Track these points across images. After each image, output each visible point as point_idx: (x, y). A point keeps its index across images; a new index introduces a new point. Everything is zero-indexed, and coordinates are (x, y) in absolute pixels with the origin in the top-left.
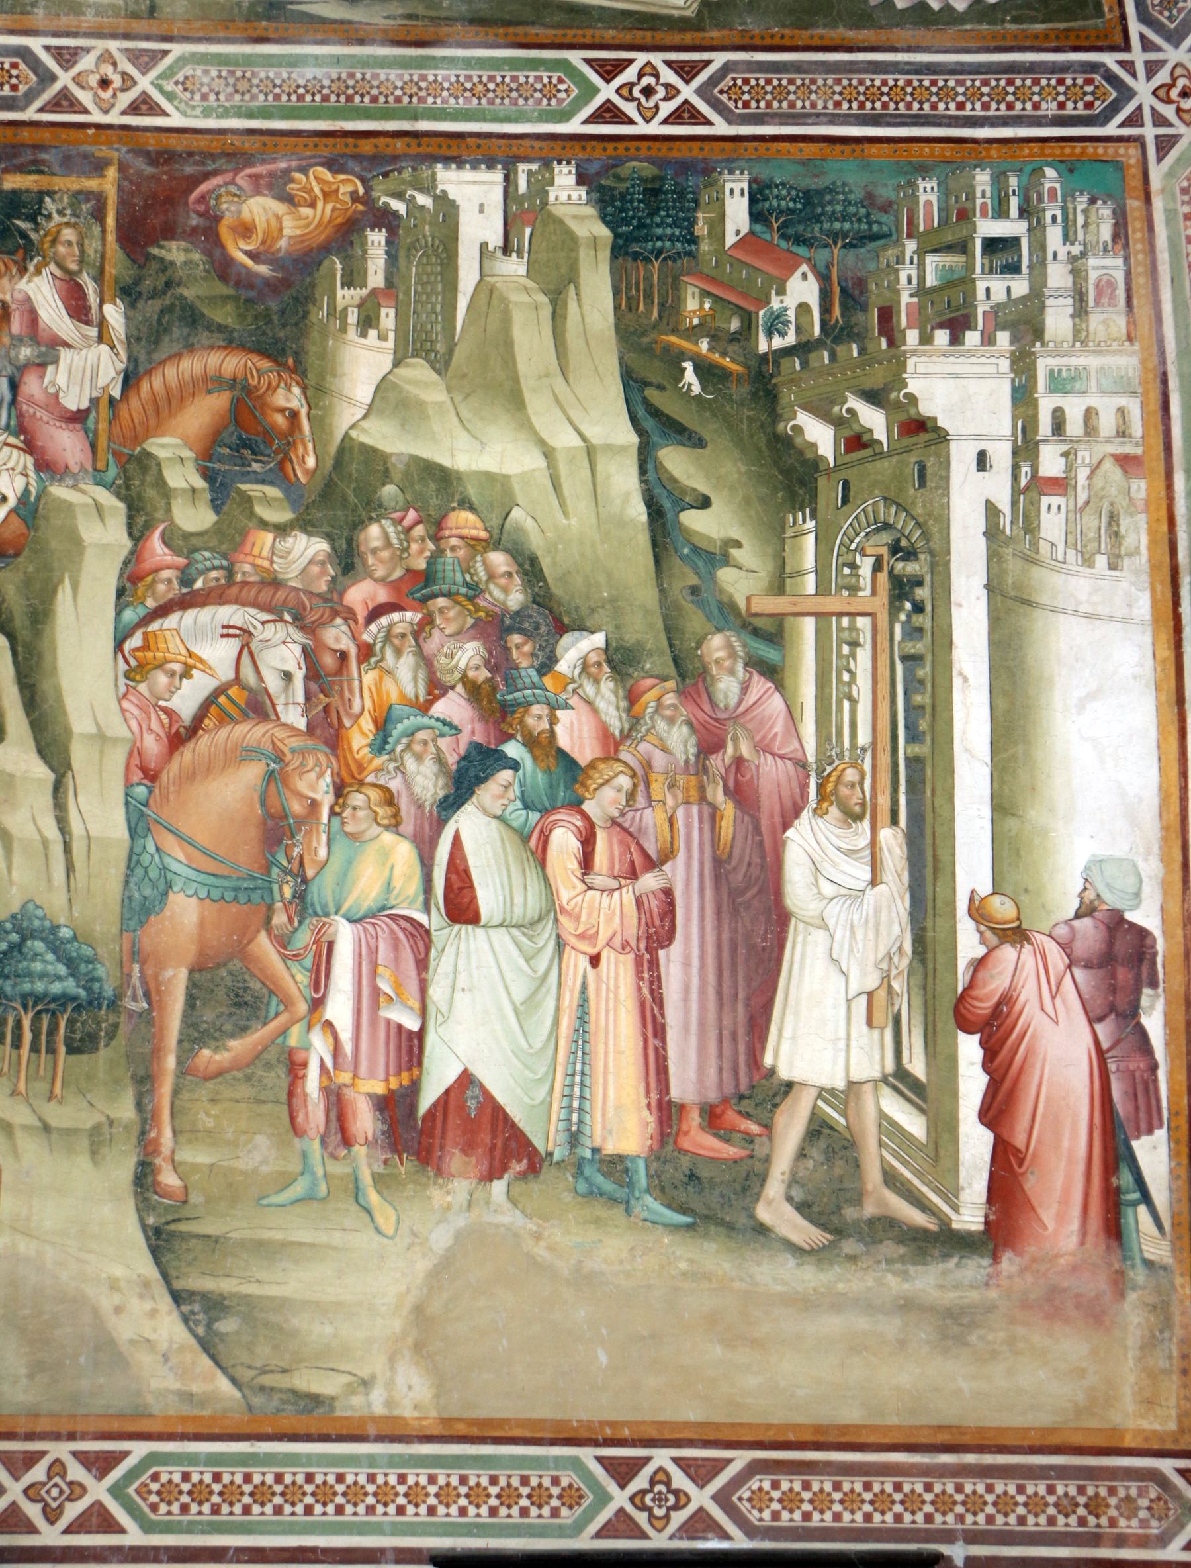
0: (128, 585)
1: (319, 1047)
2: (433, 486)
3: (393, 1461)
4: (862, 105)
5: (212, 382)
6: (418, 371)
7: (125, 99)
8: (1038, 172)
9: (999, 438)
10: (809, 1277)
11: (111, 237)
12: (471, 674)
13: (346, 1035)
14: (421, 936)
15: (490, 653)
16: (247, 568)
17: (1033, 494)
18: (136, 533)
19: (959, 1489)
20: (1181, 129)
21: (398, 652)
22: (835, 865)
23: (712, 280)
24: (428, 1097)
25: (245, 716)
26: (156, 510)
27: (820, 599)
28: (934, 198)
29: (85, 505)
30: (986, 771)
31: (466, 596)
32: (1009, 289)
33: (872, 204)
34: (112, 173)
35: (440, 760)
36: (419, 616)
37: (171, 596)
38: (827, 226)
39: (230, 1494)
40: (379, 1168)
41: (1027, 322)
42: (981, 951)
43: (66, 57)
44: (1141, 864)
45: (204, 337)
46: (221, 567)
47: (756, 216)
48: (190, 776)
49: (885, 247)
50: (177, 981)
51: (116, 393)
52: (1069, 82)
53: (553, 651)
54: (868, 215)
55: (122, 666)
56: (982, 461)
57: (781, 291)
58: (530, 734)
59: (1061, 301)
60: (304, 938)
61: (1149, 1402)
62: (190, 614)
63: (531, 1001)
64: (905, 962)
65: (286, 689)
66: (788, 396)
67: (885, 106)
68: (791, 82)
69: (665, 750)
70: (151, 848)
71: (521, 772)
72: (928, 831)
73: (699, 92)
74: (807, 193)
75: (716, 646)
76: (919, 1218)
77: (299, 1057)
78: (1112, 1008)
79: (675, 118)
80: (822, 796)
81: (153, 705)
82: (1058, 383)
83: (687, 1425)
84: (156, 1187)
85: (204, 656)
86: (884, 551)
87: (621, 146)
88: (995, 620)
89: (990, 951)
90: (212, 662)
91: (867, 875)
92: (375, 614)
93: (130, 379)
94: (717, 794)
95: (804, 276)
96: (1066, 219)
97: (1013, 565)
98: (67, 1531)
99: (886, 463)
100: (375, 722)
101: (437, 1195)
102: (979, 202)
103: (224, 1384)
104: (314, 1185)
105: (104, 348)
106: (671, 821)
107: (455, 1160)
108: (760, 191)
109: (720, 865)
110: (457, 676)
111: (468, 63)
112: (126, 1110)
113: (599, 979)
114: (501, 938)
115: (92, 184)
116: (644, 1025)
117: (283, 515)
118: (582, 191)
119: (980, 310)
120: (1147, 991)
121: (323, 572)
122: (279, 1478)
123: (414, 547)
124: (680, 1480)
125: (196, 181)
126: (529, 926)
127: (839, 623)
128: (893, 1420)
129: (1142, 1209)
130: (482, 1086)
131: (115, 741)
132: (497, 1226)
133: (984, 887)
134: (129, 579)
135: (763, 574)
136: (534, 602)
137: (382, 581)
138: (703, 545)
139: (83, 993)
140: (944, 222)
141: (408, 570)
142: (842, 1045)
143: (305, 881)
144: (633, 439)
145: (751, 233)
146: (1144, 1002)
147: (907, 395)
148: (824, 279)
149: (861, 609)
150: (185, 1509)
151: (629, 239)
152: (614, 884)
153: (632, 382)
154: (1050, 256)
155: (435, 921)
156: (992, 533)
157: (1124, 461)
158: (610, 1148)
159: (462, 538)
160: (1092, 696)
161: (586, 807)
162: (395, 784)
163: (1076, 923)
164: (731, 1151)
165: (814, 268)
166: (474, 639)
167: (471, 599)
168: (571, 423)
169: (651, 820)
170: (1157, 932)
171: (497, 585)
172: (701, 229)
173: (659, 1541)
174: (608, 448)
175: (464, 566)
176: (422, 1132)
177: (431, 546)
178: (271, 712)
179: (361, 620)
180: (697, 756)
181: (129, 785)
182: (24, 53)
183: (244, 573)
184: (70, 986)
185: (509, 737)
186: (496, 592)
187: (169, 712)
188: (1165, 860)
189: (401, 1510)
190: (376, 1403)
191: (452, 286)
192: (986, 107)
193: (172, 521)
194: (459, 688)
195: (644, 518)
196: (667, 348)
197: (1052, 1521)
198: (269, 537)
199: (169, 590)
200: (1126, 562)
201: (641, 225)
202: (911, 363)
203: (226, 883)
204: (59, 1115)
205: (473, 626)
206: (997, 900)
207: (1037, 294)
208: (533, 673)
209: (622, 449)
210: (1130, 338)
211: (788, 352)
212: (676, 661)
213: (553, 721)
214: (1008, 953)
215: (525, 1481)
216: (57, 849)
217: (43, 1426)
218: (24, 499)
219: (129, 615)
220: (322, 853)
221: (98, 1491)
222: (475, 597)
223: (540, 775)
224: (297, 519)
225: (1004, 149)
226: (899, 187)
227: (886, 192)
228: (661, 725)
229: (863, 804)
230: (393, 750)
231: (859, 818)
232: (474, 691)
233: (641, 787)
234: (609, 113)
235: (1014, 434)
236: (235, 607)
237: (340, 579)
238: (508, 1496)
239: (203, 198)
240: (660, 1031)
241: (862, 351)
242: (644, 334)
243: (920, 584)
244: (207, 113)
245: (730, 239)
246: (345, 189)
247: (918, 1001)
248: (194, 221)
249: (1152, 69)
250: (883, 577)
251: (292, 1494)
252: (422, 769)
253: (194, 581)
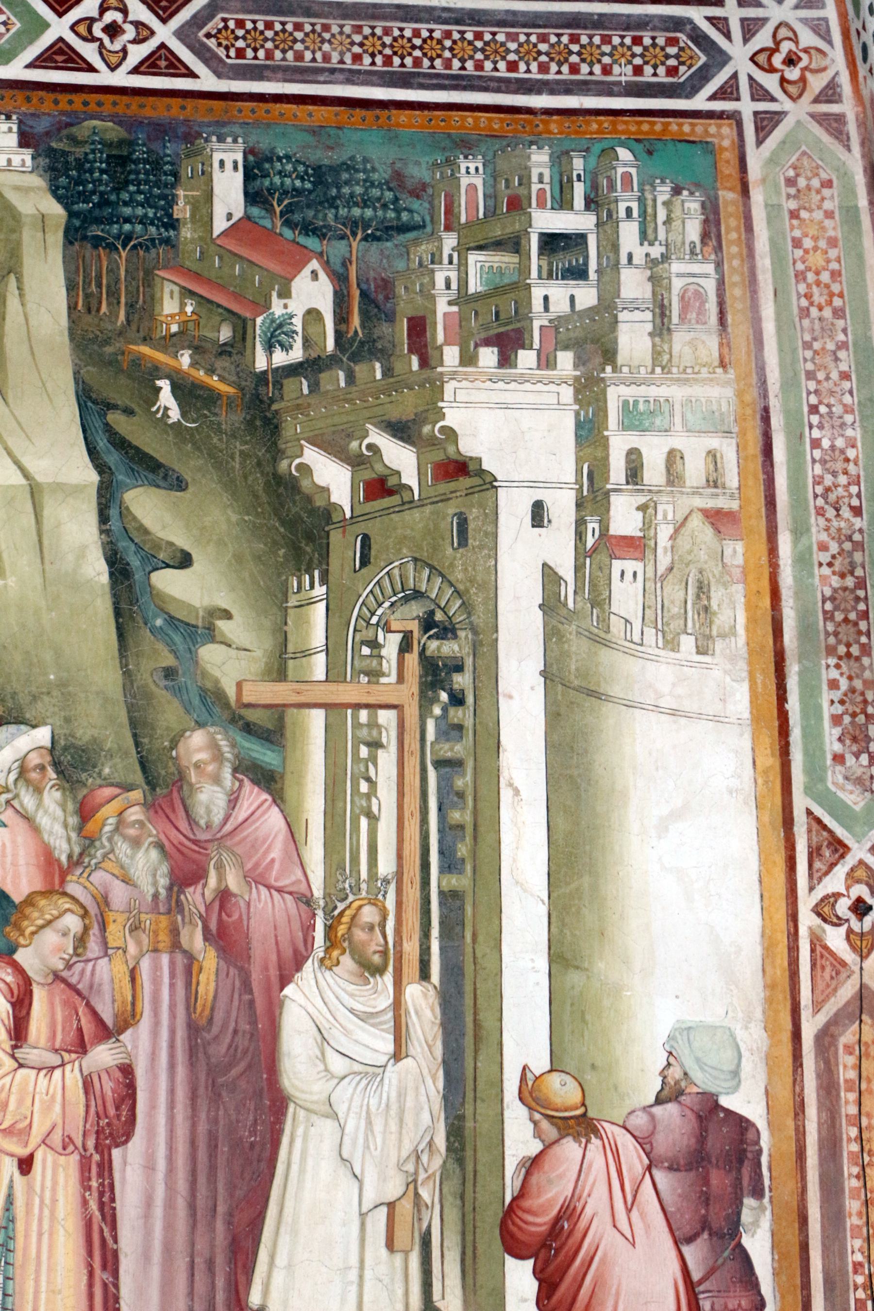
4: (388, 61)
8: (609, 153)
9: (560, 486)
17: (603, 557)
20: (786, 104)
22: (347, 1032)
23: (197, 276)
27: (332, 687)
28: (479, 182)
30: (543, 910)
32: (572, 298)
33: (402, 186)
38: (343, 212)
41: (596, 341)
42: (536, 1147)
44: (741, 1035)
47: (252, 197)
49: (416, 242)
52: (647, 41)
54: (396, 199)
57: (285, 293)
59: (637, 315)
64: (437, 1163)
67: (417, 62)
68: (298, 27)
69: (127, 880)
72: (468, 988)
73: (179, 34)
74: (317, 169)
78: (704, 1225)
79: (147, 66)
86: (414, 626)
87: (78, 98)
89: (548, 1147)
91: (390, 1048)
95: (315, 275)
96: (643, 213)
97: (578, 647)
99: (416, 514)
102: (535, 188)
108: (258, 165)
113: (30, 1188)
116: (90, 1253)
118: (26, 156)
119: (536, 324)
120: (749, 1202)
127: (355, 717)
133: (540, 1063)
135: (259, 653)
138: (180, 615)
140: (491, 212)
142: (353, 1275)
144: (93, 477)
145: (247, 217)
146: (746, 1216)
147: (443, 429)
148: (339, 279)
149: (383, 700)
151: (88, 219)
152: (55, 1060)
154: (624, 260)
160: (676, 815)
161: (20, 956)
163: (658, 1110)
165: (327, 265)
168: (10, 453)
170: (761, 1124)
172: (182, 210)
174: (59, 488)
180: (170, 889)
188: (771, 1027)
192: (544, 68)
195: (105, 579)
196: (137, 361)
200: (719, 645)
201: (104, 202)
202: (449, 388)
206: (556, 1079)
209: (77, 490)
210: (723, 364)
211: (293, 370)
212: (144, 765)
214: (570, 1149)
225: (567, 122)
226: (435, 165)
228: (123, 848)
229: (384, 953)
231: (379, 971)
233: (95, 930)
235: (579, 481)
241: (388, 372)
242: (107, 342)
243: (459, 668)
245: (220, 225)
247: (453, 1215)
249: (750, 28)
250: (412, 659)
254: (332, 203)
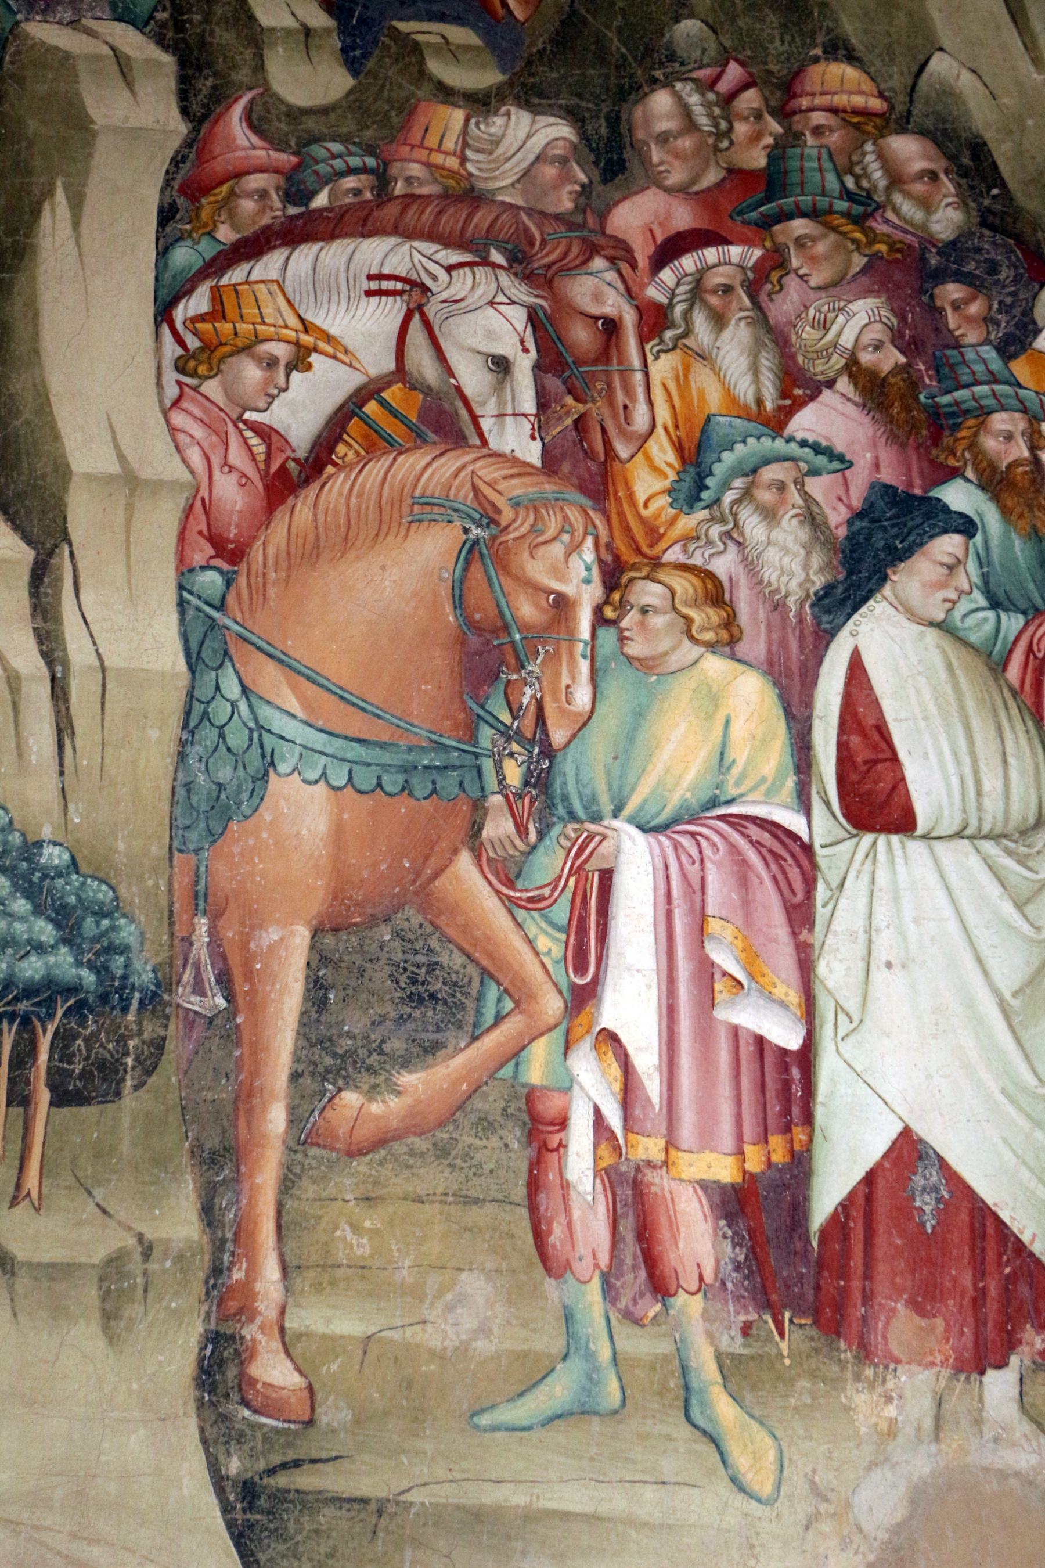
0: (181, 201)
2: (773, 18)
12: (866, 358)
15: (902, 319)
16: (415, 169)
18: (196, 109)
21: (719, 320)
25: (419, 439)
26: (234, 67)
29: (97, 58)
31: (847, 215)
35: (812, 517)
36: (757, 253)
37: (266, 220)
40: (733, 1343)
46: (364, 170)
53: (1028, 312)
55: (171, 349)
58: (992, 466)
62: (304, 257)
65: (499, 387)
70: (232, 689)
71: (979, 538)
77: (549, 1107)
85: (333, 331)
90: (348, 341)
100: (679, 448)
104: (592, 1380)
110: (838, 362)
121: (566, 177)
123: (741, 129)
130: (943, 1165)
131: (157, 486)
132: (1003, 1475)
134: (182, 191)
136: (983, 224)
137: (682, 191)
139: (89, 978)
141: (732, 171)
143: (548, 752)
159: (834, 111)
166: (867, 293)
167: (859, 221)
171: (908, 195)
175: (842, 161)
176: (821, 1265)
177: (774, 126)
178: (470, 431)
179: (643, 261)
181: (185, 570)
183: (409, 180)
186: (907, 207)
187: (265, 433)
193: (267, 88)
194: (843, 384)
198: (458, 116)
199: (262, 211)
203: (386, 758)
205: (864, 271)
208: (989, 353)
216: (38, 694)
219: (183, 256)
220: (582, 696)
222: (866, 216)
223: (1018, 544)
224: (511, 83)
230: (717, 501)
236: (393, 240)
237: (599, 188)
252: (777, 535)
253: (313, 194)
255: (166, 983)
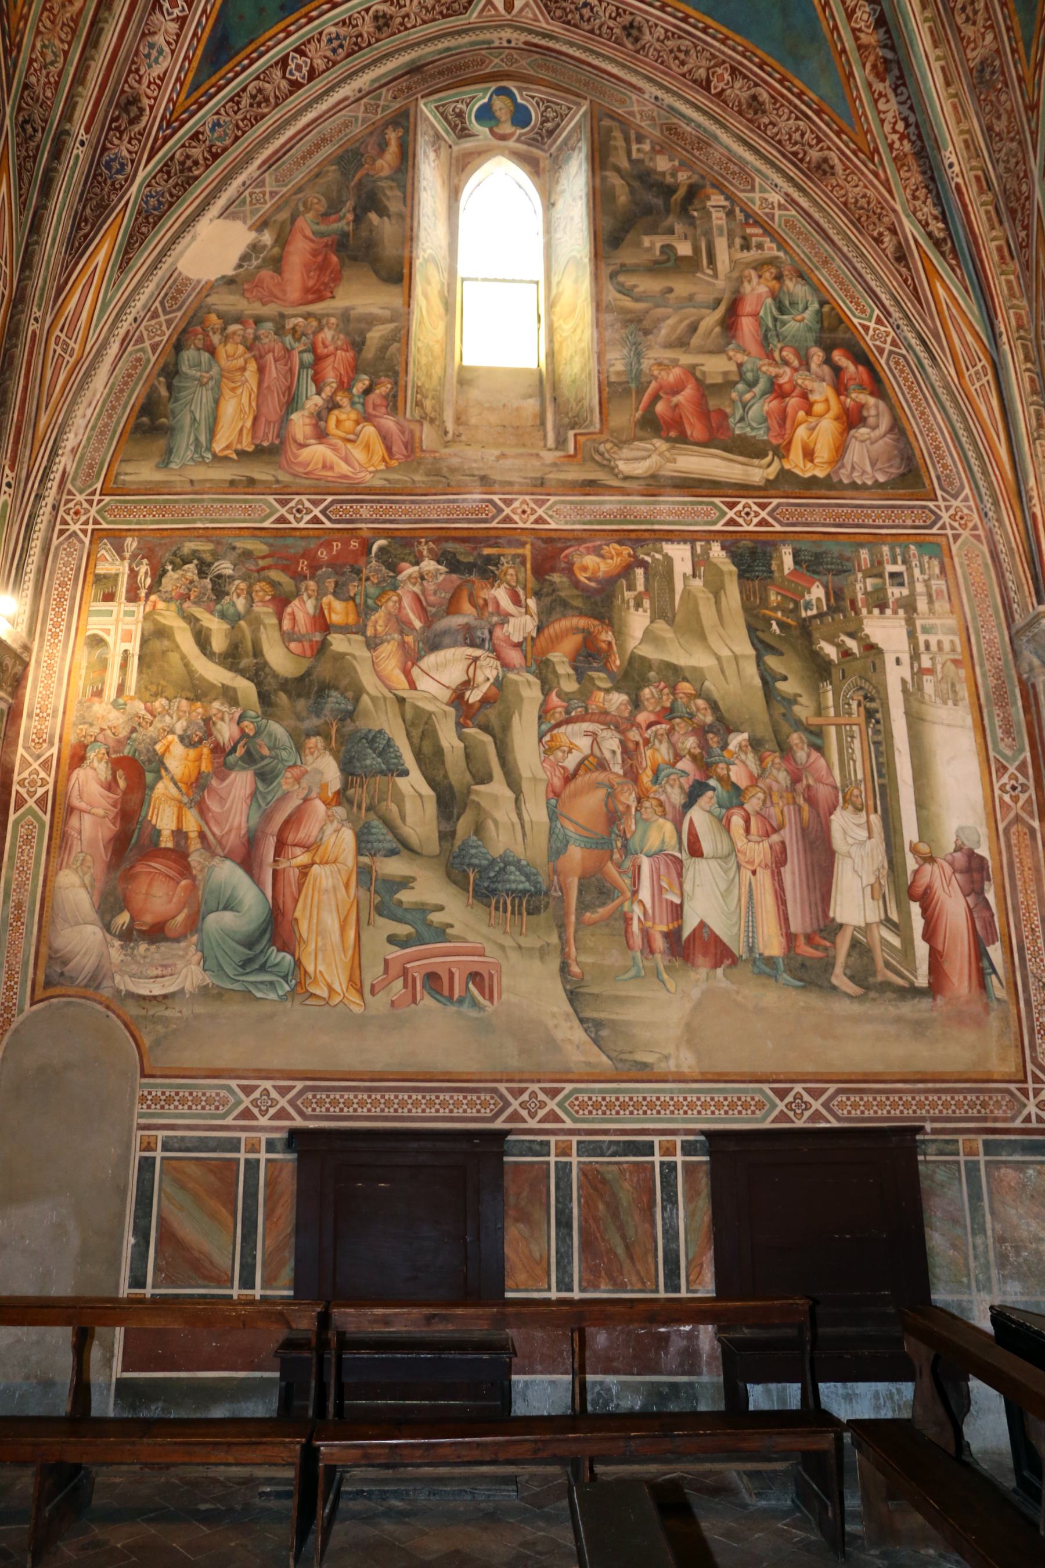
1: (637, 911)
3: (681, 1091)
5: (576, 630)
6: (661, 625)
7: (533, 518)
8: (907, 547)
10: (856, 1008)
11: (529, 572)
13: (649, 906)
14: (678, 863)
19: (927, 1099)
20: (961, 531)
21: (661, 742)
24: (686, 932)
25: (597, 769)
34: (528, 546)
35: (681, 787)
39: (610, 1106)
40: (667, 963)
42: (916, 866)
43: (508, 503)
45: (570, 612)
47: (797, 562)
48: (574, 795)
50: (574, 884)
51: (534, 635)
56: (898, 661)
60: (628, 864)
61: (1003, 1059)
62: (570, 727)
63: (728, 890)
64: (885, 872)
66: (816, 635)
75: (795, 738)
76: (900, 982)
78: (973, 890)
79: (760, 524)
80: (845, 801)
81: (556, 765)
82: (926, 630)
83: (808, 1073)
84: (569, 973)
88: (910, 727)
91: (865, 834)
92: (650, 726)
93: (540, 629)
94: (801, 801)
97: (915, 704)
98: (540, 1122)
101: (693, 975)
103: (604, 1058)
104: (639, 971)
105: (528, 617)
106: (782, 812)
107: (700, 960)
109: (804, 831)
111: (673, 503)
112: (554, 939)
114: (713, 863)
115: (520, 551)
117: (607, 685)
118: (724, 553)
120: (986, 883)
122: (631, 1099)
124: (807, 1097)
125: (563, 549)
126: (725, 858)
128: (897, 1070)
129: (993, 977)
131: (541, 780)
133: (916, 839)
137: (652, 712)
140: (872, 565)
144: (753, 652)
146: (986, 887)
148: (826, 587)
150: (590, 1112)
153: (752, 630)
155: (684, 856)
156: (905, 691)
157: (955, 662)
158: (767, 953)
161: (746, 806)
162: (663, 798)
164: (819, 954)
169: (774, 812)
172: (774, 567)
173: (799, 1124)
181: (548, 799)
182: (491, 501)
184: (527, 885)
185: (710, 777)
187: (563, 768)
188: (988, 827)
189: (686, 1112)
190: (672, 1065)
191: (672, 590)
196: (764, 615)
197: (966, 1112)
198: (602, 694)
204: (525, 942)
207: (913, 594)
211: (814, 617)
212: (779, 744)
213: (728, 770)
214: (928, 867)
215: (739, 1099)
216: (518, 827)
217: (525, 1077)
218: (497, 679)
219: (544, 727)
220: (633, 827)
221: (552, 1105)
227: (848, 553)
228: (775, 772)
231: (861, 810)
232: (694, 758)
234: (732, 522)
238: (732, 1106)
239: (566, 556)
240: (784, 902)
244: (566, 523)
245: (786, 572)
246: (625, 552)
247: (892, 887)
248: (563, 565)
249: (948, 508)
250: (862, 709)
251: (637, 1106)
254: (821, 564)
255: (549, 890)
